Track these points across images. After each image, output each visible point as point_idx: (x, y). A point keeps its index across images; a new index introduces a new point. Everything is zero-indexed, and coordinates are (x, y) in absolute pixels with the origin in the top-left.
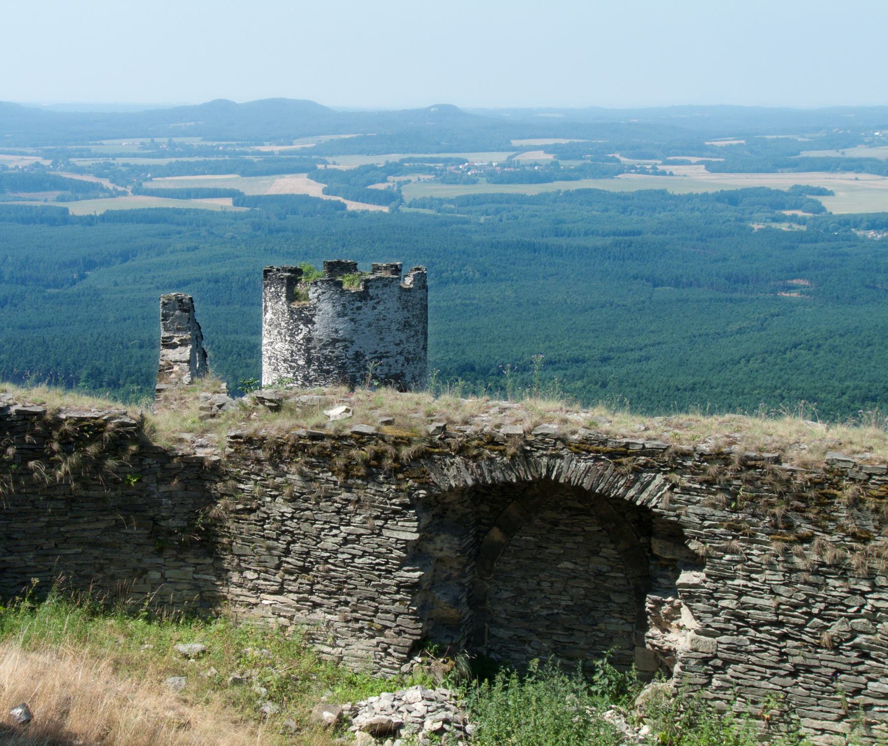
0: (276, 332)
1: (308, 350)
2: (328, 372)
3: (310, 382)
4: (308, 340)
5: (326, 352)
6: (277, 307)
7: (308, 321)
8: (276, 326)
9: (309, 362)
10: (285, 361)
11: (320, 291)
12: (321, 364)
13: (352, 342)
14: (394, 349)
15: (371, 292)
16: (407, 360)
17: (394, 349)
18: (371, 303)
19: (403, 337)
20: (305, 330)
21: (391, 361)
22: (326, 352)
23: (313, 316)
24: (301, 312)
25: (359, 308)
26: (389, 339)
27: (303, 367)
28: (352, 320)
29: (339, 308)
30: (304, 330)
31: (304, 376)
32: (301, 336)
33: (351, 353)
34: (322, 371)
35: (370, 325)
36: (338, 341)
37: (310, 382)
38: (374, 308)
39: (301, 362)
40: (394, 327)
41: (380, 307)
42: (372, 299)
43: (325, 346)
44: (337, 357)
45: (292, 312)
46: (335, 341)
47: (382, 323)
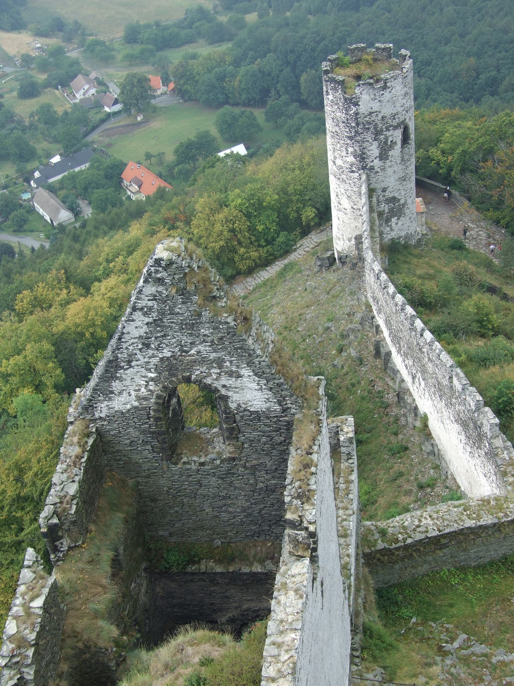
0: (336, 107)
1: (356, 119)
2: (368, 129)
3: (359, 134)
4: (357, 114)
5: (367, 119)
6: (336, 94)
7: (356, 104)
8: (336, 104)
9: (358, 124)
10: (343, 122)
11: (362, 89)
12: (364, 125)
13: (380, 112)
14: (400, 109)
15: (388, 85)
16: (407, 111)
17: (400, 109)
18: (389, 90)
19: (404, 101)
20: (354, 109)
21: (399, 116)
22: (367, 119)
23: (358, 101)
24: (351, 100)
25: (382, 94)
26: (398, 105)
27: (354, 127)
28: (380, 101)
29: (373, 96)
30: (354, 109)
31: (355, 131)
32: (352, 112)
33: (380, 117)
34: (365, 129)
35: (389, 101)
36: (373, 113)
37: (359, 134)
38: (390, 92)
39: (353, 125)
40: (400, 98)
41: (393, 91)
42: (389, 88)
43: (366, 117)
44: (373, 121)
45: (345, 99)
46: (371, 113)
47: (394, 99)
